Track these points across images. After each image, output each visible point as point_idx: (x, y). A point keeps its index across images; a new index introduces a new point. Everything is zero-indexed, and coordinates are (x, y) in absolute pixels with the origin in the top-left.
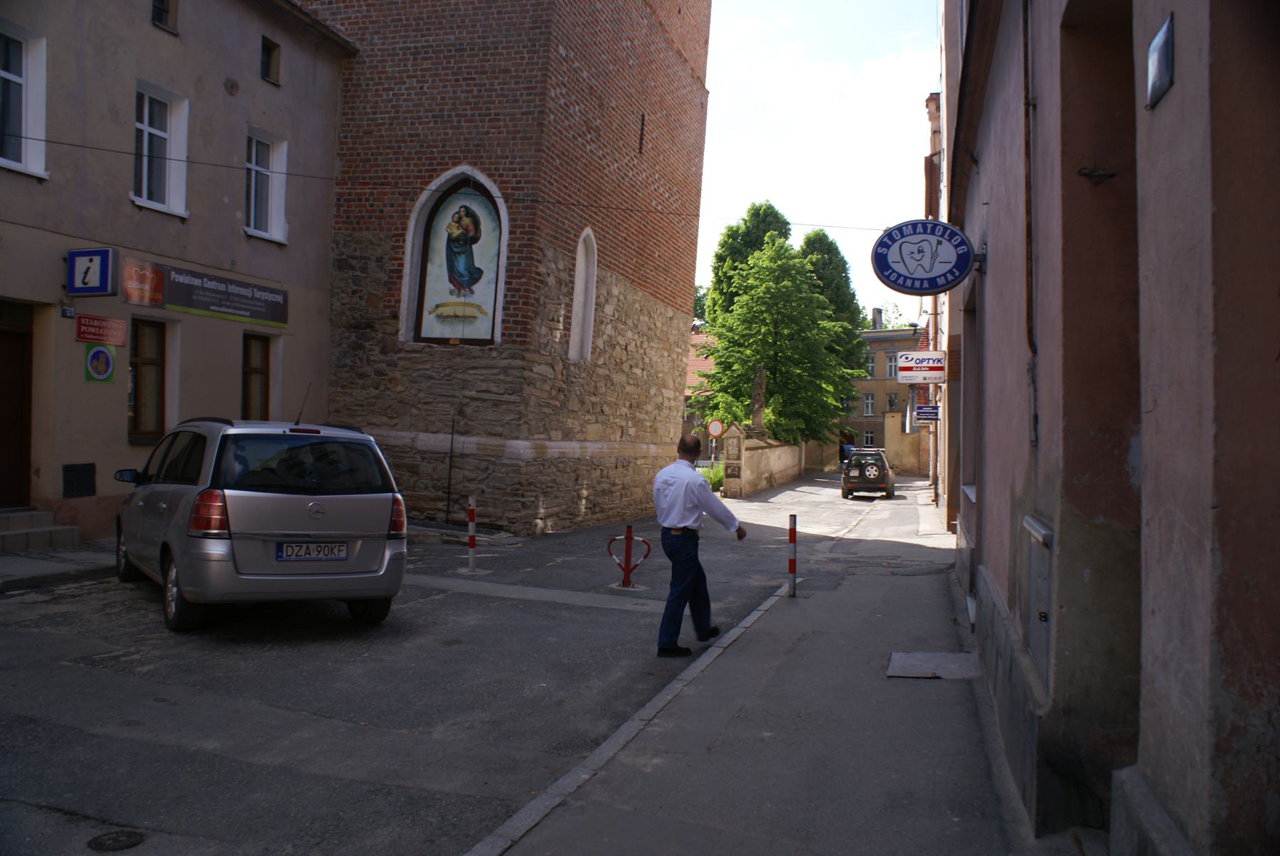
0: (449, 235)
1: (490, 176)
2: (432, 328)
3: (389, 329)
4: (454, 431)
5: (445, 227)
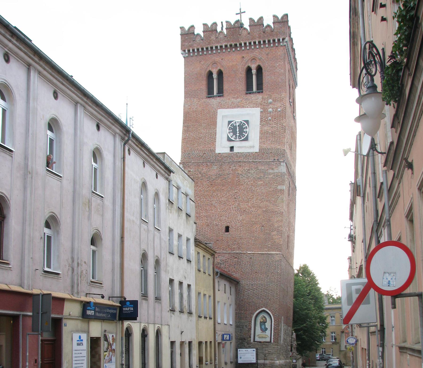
0: (260, 322)
1: (269, 310)
2: (257, 339)
3: (249, 340)
4: (265, 360)
5: (259, 319)
